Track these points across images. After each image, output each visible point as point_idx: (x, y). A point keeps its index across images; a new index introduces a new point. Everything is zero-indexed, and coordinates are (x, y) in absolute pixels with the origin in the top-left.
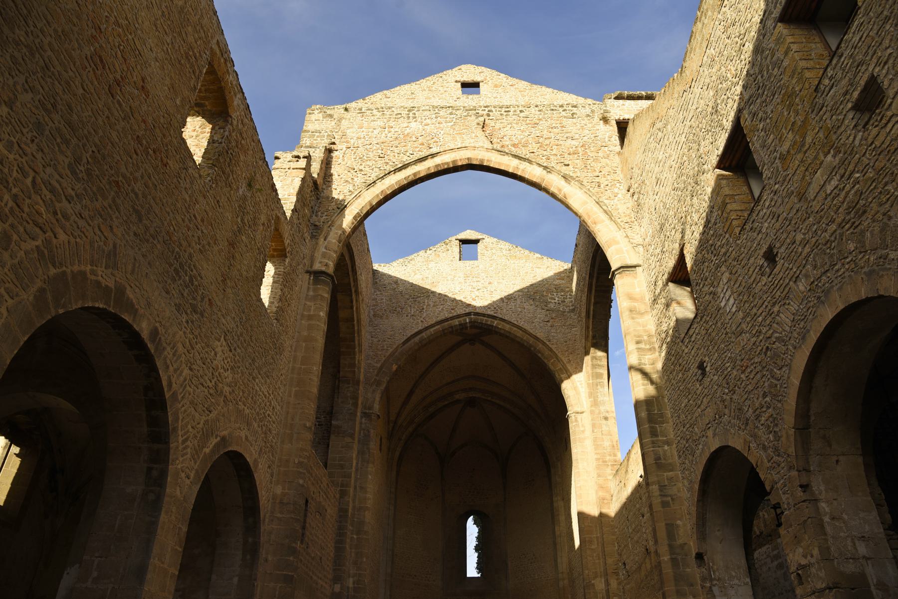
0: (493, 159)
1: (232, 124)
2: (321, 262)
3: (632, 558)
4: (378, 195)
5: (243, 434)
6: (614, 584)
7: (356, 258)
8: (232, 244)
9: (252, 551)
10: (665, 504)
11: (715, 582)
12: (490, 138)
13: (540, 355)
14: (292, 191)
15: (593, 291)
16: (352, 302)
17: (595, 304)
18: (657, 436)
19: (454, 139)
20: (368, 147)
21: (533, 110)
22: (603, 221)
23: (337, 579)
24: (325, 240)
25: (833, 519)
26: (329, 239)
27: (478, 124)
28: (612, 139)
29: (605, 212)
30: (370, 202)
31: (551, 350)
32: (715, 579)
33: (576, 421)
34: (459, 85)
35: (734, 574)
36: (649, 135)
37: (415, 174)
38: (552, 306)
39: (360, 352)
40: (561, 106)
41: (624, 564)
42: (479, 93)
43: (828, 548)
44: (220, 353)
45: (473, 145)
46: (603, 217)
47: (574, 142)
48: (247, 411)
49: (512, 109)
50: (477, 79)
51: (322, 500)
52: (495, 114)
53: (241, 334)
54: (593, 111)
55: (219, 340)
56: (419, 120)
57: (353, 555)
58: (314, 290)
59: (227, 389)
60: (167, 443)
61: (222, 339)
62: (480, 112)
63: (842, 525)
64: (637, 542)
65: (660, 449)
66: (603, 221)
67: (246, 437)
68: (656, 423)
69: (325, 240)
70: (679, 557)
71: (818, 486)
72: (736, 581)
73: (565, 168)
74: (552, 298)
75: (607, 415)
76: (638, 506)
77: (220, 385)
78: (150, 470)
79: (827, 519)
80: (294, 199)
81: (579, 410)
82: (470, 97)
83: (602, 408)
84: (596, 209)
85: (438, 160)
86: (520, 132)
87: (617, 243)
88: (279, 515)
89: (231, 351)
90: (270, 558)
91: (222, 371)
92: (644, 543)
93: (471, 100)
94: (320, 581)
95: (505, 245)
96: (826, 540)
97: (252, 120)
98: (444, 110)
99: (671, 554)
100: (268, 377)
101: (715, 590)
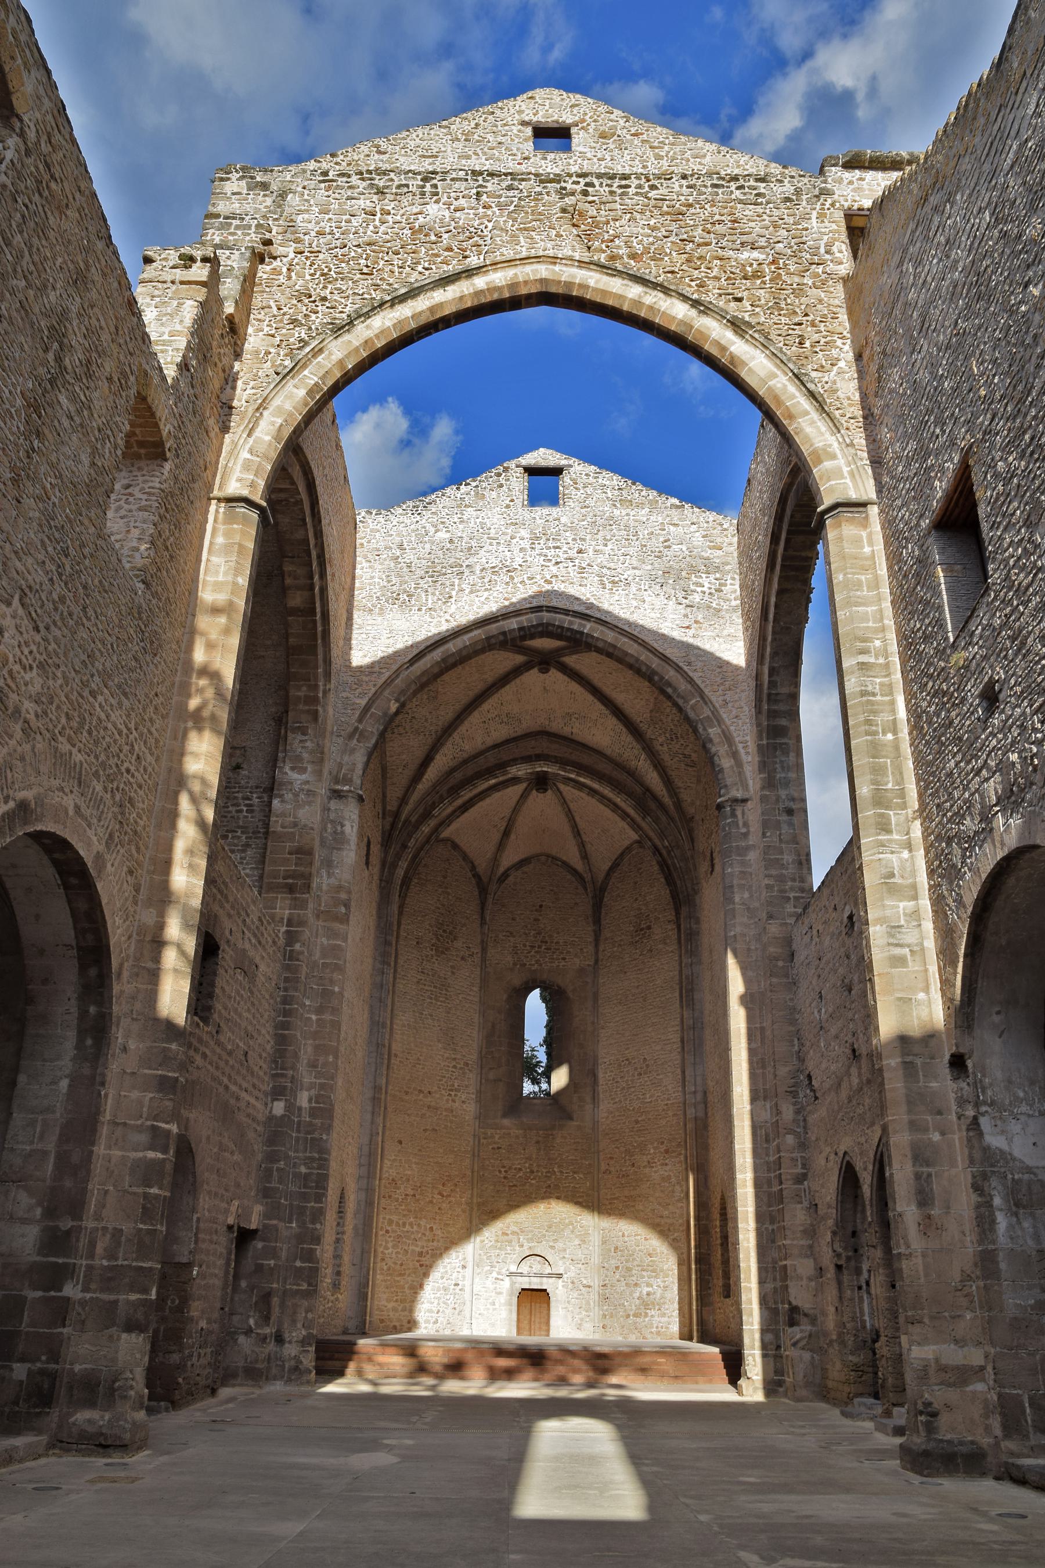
0: (592, 283)
1: (22, 135)
2: (239, 480)
3: (824, 1066)
4: (357, 349)
5: (69, 802)
6: (788, 1112)
7: (320, 490)
8: (34, 406)
11: (983, 1109)
12: (586, 240)
13: (669, 690)
14: (178, 327)
15: (778, 568)
16: (312, 578)
17: (780, 592)
18: (889, 831)
19: (514, 239)
20: (340, 252)
21: (676, 184)
22: (807, 413)
24: (249, 435)
26: (258, 433)
27: (564, 210)
28: (835, 249)
29: (812, 395)
30: (341, 363)
31: (691, 681)
32: (985, 1103)
33: (733, 814)
34: (529, 131)
35: (1021, 1094)
36: (912, 226)
37: (432, 309)
38: (697, 598)
39: (328, 675)
40: (735, 179)
41: (809, 1077)
42: (568, 149)
44: (13, 631)
45: (551, 253)
46: (804, 403)
47: (755, 254)
48: (78, 757)
49: (634, 182)
50: (567, 118)
51: (247, 946)
52: (601, 189)
53: (62, 599)
54: (798, 192)
55: (9, 604)
56: (445, 199)
57: (309, 1049)
58: (226, 535)
59: (28, 706)
61: (16, 601)
62: (569, 186)
64: (837, 1037)
65: (894, 858)
66: (807, 413)
67: (77, 808)
68: (887, 808)
69: (249, 435)
70: (919, 1061)
72: (1024, 1108)
73: (733, 304)
74: (697, 584)
75: (792, 805)
76: (841, 971)
77: (14, 696)
80: (182, 343)
81: (739, 795)
82: (551, 156)
83: (783, 793)
84: (792, 389)
85: (480, 282)
86: (647, 231)
87: (834, 457)
89: (37, 629)
90: (132, 1045)
91: (17, 667)
92: (849, 1038)
93: (551, 163)
94: (243, 1094)
95: (611, 480)
97: (74, 141)
98: (496, 180)
99: (904, 1054)
100: (125, 694)
101: (985, 1122)
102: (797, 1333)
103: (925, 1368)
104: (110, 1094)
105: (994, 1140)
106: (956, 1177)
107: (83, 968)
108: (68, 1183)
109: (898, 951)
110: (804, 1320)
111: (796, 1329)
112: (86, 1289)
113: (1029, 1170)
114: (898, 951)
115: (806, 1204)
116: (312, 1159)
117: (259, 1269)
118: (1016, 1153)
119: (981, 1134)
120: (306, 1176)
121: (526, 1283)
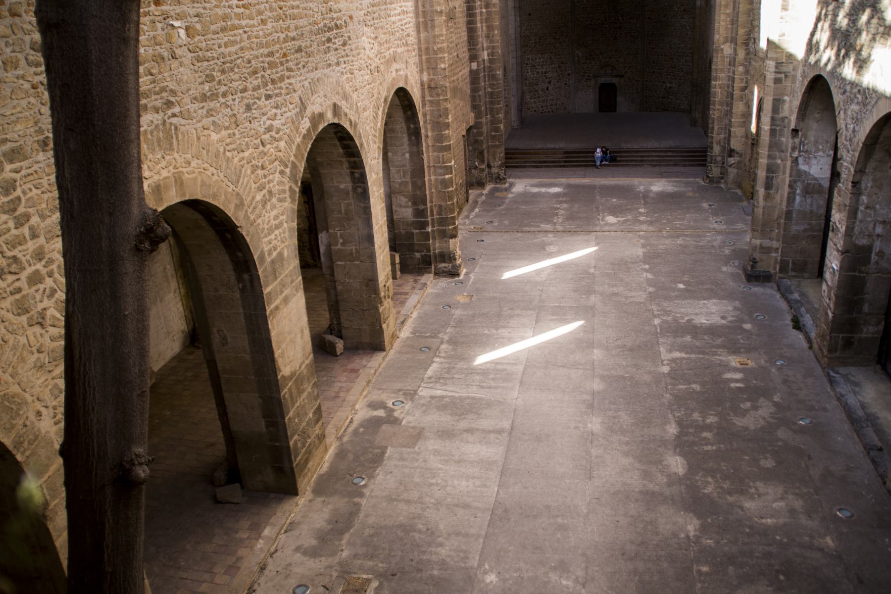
9: (415, 134)
10: (777, 81)
23: (473, 58)
25: (867, 207)
35: (821, 147)
43: (853, 228)
57: (484, 28)
60: (361, 157)
63: (872, 212)
70: (778, 128)
71: (867, 183)
72: (821, 153)
78: (352, 174)
79: (862, 208)
88: (430, 98)
90: (430, 134)
96: (854, 223)
101: (800, 160)
102: (732, 160)
103: (756, 247)
104: (425, 157)
105: (803, 167)
106: (784, 179)
107: (405, 112)
108: (418, 193)
109: (779, 76)
110: (736, 155)
111: (732, 159)
112: (433, 226)
113: (816, 179)
114: (779, 76)
115: (745, 101)
116: (493, 85)
117: (476, 141)
118: (812, 172)
119: (798, 164)
120: (491, 94)
121: (602, 80)
